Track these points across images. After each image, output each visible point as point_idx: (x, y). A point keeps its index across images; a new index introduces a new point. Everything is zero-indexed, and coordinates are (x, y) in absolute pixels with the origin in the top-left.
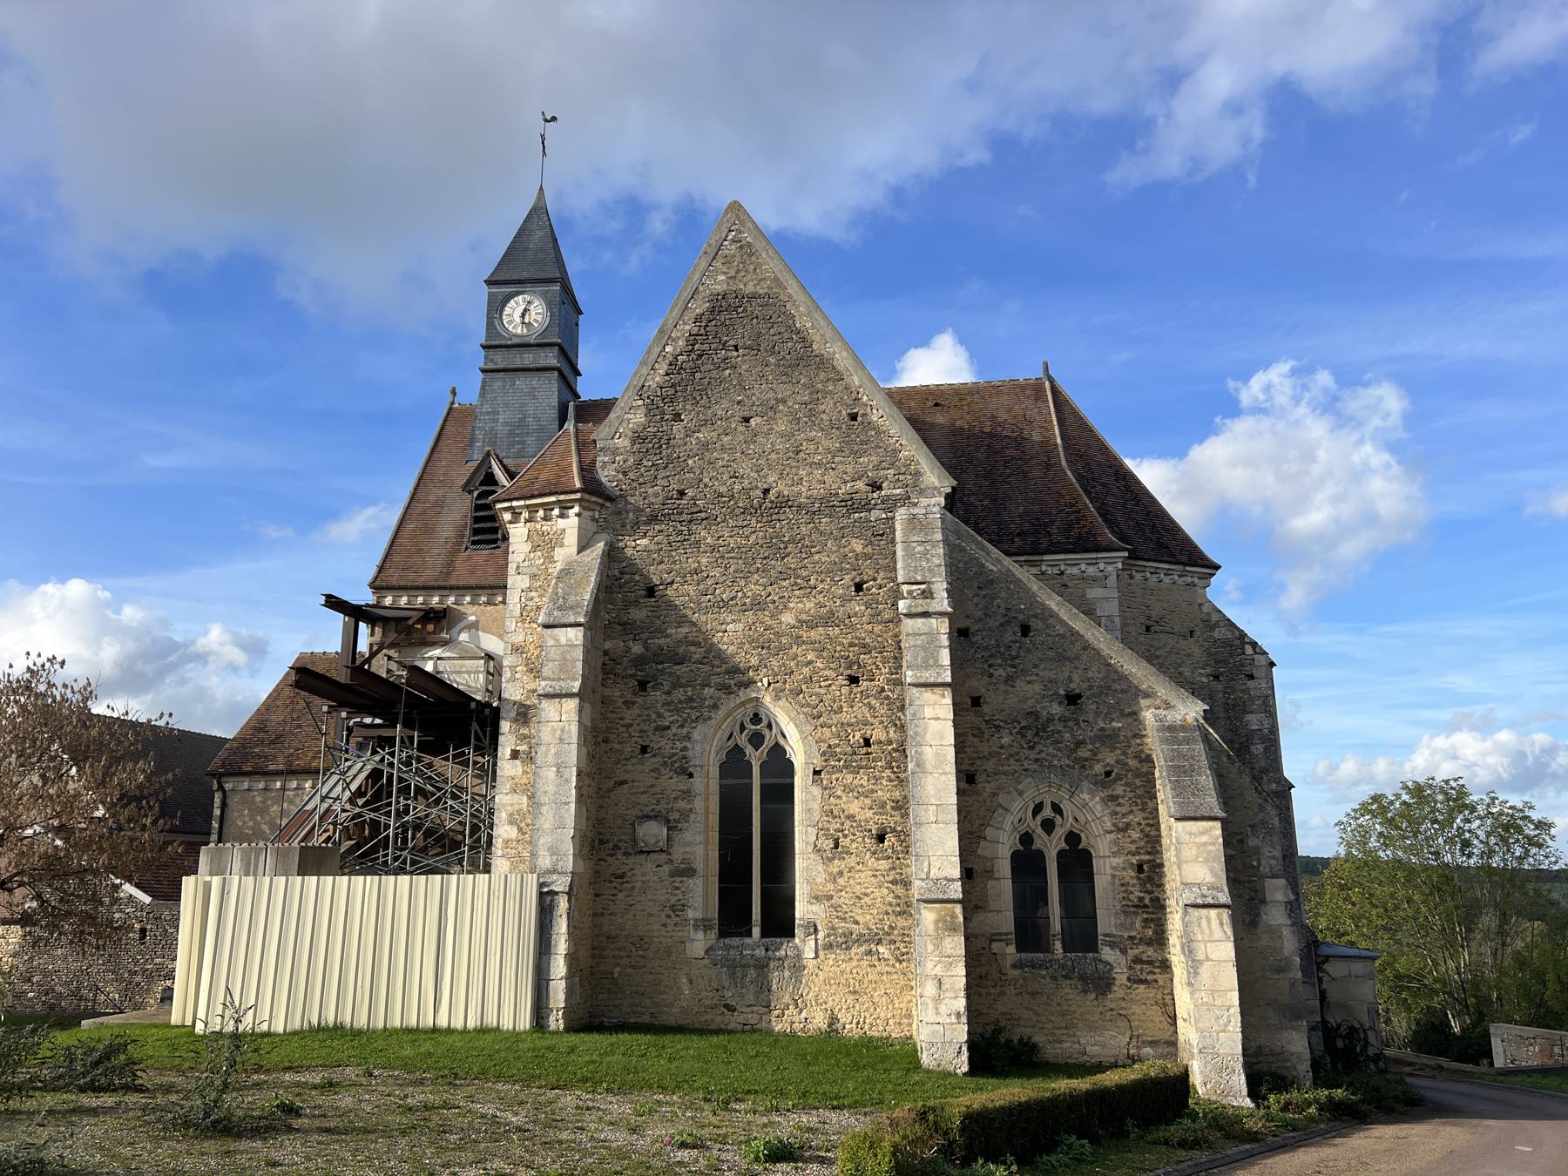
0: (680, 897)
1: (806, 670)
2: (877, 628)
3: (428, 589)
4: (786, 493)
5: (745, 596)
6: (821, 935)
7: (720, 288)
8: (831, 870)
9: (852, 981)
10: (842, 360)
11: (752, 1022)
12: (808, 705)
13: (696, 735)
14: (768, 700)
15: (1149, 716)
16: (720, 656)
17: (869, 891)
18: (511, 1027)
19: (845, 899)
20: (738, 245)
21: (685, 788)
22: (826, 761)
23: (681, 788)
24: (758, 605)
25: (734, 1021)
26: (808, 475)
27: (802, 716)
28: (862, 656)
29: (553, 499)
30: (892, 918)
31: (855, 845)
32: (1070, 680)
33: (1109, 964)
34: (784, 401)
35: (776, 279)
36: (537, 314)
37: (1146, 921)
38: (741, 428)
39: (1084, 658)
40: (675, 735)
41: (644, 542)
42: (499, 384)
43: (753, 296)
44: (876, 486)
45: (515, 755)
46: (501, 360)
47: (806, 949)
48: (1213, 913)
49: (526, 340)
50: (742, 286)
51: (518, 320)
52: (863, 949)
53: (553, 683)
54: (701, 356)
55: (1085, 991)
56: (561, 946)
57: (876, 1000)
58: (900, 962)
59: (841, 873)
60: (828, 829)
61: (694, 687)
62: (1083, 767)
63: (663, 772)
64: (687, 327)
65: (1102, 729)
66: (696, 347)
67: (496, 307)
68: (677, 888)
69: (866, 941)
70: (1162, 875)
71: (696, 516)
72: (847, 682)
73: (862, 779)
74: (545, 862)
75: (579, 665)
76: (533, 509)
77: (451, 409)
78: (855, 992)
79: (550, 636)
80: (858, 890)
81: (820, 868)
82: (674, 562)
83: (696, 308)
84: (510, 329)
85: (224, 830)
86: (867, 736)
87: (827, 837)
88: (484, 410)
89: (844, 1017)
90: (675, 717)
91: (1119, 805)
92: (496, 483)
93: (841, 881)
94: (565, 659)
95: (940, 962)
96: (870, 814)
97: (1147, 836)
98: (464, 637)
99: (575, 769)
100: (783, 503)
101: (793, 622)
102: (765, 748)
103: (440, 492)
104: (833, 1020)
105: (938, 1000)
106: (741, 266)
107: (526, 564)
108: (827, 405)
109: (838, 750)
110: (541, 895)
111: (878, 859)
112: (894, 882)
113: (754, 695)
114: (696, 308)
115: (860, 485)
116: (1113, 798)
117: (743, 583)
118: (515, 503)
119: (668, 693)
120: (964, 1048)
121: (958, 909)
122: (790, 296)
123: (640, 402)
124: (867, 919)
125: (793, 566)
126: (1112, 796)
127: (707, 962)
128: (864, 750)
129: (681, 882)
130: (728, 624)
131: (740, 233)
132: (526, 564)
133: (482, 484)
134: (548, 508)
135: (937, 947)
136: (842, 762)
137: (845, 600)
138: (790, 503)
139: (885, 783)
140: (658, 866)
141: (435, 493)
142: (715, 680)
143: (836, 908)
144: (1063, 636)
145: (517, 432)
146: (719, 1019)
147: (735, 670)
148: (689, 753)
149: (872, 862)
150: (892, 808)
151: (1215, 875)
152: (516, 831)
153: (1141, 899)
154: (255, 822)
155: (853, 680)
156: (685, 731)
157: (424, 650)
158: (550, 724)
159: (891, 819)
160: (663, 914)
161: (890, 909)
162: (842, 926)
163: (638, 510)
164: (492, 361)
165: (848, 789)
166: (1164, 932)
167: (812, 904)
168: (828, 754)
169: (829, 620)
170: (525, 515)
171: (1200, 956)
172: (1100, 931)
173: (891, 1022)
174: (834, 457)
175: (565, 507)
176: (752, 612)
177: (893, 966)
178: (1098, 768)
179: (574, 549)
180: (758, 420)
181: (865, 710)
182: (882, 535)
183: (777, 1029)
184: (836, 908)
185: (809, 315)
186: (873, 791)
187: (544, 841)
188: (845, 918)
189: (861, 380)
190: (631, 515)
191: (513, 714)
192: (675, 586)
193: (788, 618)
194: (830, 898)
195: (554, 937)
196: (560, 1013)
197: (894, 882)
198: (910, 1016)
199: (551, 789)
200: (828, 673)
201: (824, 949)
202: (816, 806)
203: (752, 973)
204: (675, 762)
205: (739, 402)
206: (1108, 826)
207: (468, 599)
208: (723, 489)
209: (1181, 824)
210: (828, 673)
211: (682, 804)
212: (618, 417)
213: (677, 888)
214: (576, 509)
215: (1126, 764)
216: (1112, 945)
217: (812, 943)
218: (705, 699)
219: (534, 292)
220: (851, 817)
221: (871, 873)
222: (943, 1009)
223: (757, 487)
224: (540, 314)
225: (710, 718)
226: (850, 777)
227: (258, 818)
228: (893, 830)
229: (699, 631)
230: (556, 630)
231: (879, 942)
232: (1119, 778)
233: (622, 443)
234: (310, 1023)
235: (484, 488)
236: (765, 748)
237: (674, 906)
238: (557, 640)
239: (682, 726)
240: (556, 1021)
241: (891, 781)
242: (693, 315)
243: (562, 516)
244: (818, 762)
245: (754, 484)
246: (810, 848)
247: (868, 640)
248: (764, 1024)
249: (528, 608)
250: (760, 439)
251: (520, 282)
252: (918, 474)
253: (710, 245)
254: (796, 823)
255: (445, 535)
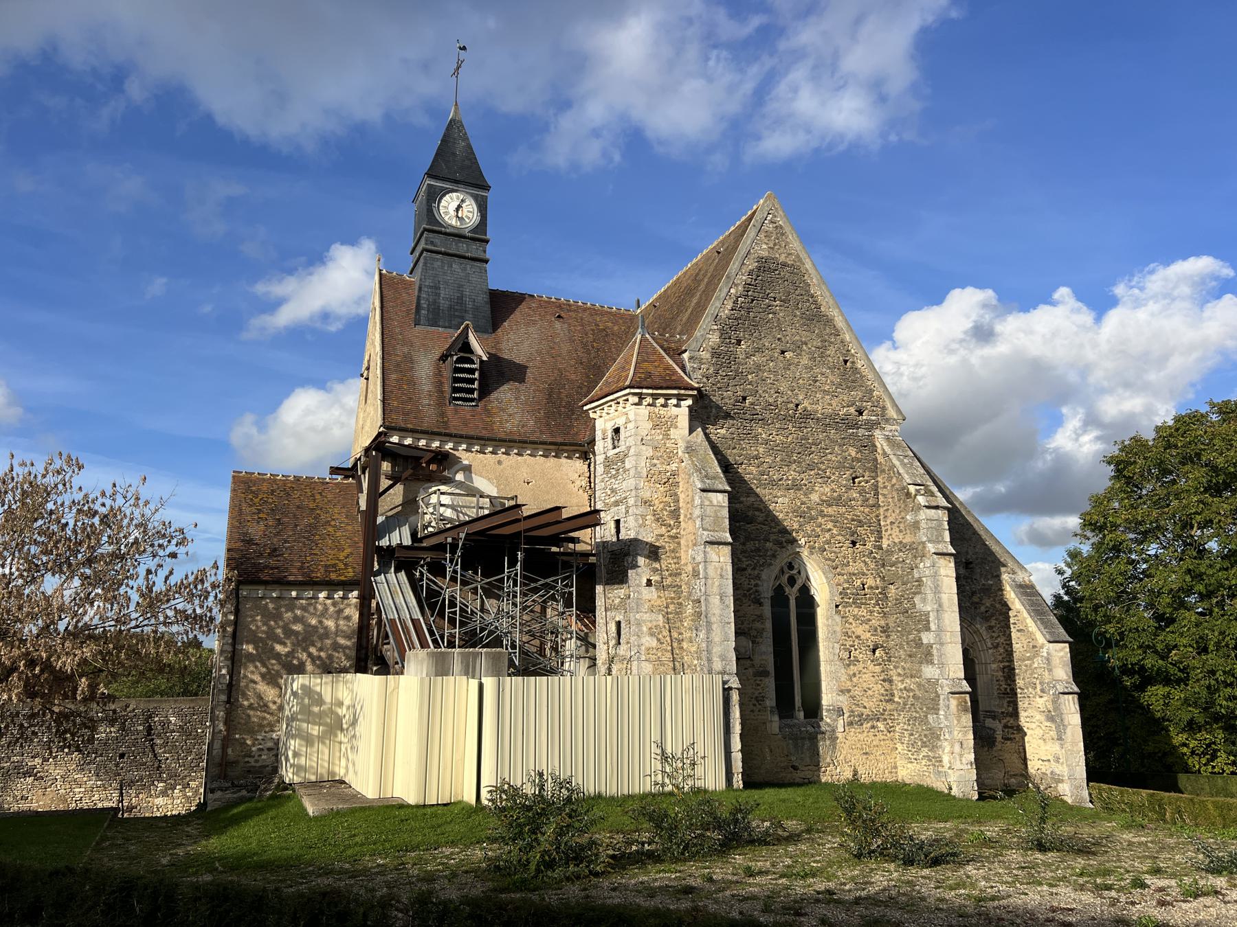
0: (761, 691)
1: (827, 535)
2: (867, 510)
3: (431, 434)
4: (809, 409)
5: (788, 479)
6: (846, 716)
7: (765, 254)
8: (848, 672)
9: (864, 746)
10: (839, 322)
11: (808, 777)
12: (830, 559)
13: (764, 577)
14: (805, 553)
15: (1005, 577)
16: (775, 520)
17: (871, 686)
18: (714, 789)
19: (857, 692)
20: (775, 225)
21: (758, 613)
22: (842, 598)
23: (756, 613)
24: (796, 486)
25: (798, 776)
26: (822, 398)
27: (827, 567)
28: (859, 528)
29: (675, 392)
30: (884, 704)
31: (861, 656)
32: (967, 553)
33: (991, 729)
34: (806, 344)
35: (798, 256)
36: (468, 211)
37: (1009, 702)
38: (781, 358)
39: (974, 539)
40: (750, 575)
41: (723, 431)
42: (439, 263)
43: (784, 265)
44: (861, 413)
45: (649, 583)
46: (440, 244)
47: (839, 726)
48: (1071, 696)
49: (461, 232)
50: (778, 256)
51: (453, 213)
52: (869, 725)
53: (712, 533)
54: (753, 300)
55: (983, 746)
56: (737, 728)
57: (878, 758)
58: (890, 732)
59: (854, 675)
60: (846, 645)
61: (759, 541)
62: (976, 608)
63: (744, 601)
64: (744, 278)
65: (984, 585)
66: (750, 293)
67: (434, 196)
68: (758, 685)
69: (872, 719)
70: (1014, 675)
71: (755, 418)
72: (851, 545)
73: (863, 612)
74: (718, 665)
75: (727, 522)
76: (655, 397)
77: (381, 274)
78: (866, 753)
79: (706, 498)
80: (865, 685)
81: (843, 671)
82: (742, 449)
83: (749, 265)
84: (446, 219)
85: (238, 634)
86: (864, 582)
87: (846, 650)
88: (427, 284)
89: (861, 771)
90: (750, 562)
91: (994, 632)
92: (472, 352)
93: (855, 679)
94: (717, 516)
95: (960, 731)
96: (868, 635)
97: (1007, 651)
98: (460, 477)
99: (732, 598)
100: (807, 415)
101: (818, 500)
102: (797, 587)
103: (406, 350)
104: (855, 773)
105: (961, 755)
106: (777, 241)
107: (649, 438)
108: (831, 351)
109: (849, 591)
110: (724, 689)
111: (875, 665)
112: (884, 680)
113: (798, 550)
114: (749, 265)
115: (852, 410)
116: (991, 628)
117: (786, 469)
118: (645, 391)
119: (744, 544)
120: (975, 784)
121: (968, 697)
122: (807, 270)
123: (716, 327)
124: (871, 705)
125: (816, 461)
126: (990, 626)
127: (780, 736)
128: (863, 592)
129: (761, 680)
130: (779, 498)
131: (775, 216)
132: (649, 438)
133: (460, 350)
134: (667, 397)
135: (958, 721)
136: (851, 600)
137: (849, 489)
138: (812, 416)
139: (876, 614)
140: (746, 669)
141: (401, 350)
142: (772, 537)
143: (853, 697)
144: (963, 525)
145: (456, 307)
146: (789, 776)
147: (785, 531)
148: (760, 589)
149: (871, 667)
150: (881, 631)
151: (1067, 675)
152: (656, 642)
153: (1006, 689)
154: (269, 627)
155: (854, 543)
156: (756, 572)
157: (426, 485)
158: (714, 564)
159: (880, 639)
160: (751, 703)
161: (882, 698)
162: (858, 710)
163: (719, 408)
164: (432, 243)
165: (856, 618)
166: (1017, 708)
167: (839, 695)
168: (843, 594)
169: (837, 501)
170: (649, 400)
171: (1066, 723)
172: (981, 708)
173: (886, 771)
174: (836, 388)
175: (680, 398)
176: (792, 491)
177: (886, 735)
178: (983, 609)
179: (687, 431)
180: (792, 354)
181: (863, 565)
182: (865, 447)
183: (823, 781)
184: (853, 697)
185: (819, 286)
186: (870, 620)
187: (716, 650)
188: (858, 705)
189: (850, 338)
190: (714, 410)
191: (646, 552)
192: (743, 466)
193: (815, 497)
194: (849, 691)
195: (732, 721)
196: (740, 776)
197: (884, 680)
198: (896, 767)
199: (717, 612)
200: (840, 538)
201: (848, 725)
202: (838, 629)
203: (807, 743)
204: (751, 594)
205: (779, 339)
206: (989, 645)
207: (464, 446)
208: (771, 400)
209: (1051, 645)
210: (840, 538)
211: (758, 625)
212: (702, 335)
213: (758, 685)
214: (689, 402)
215: (995, 607)
216: (994, 718)
217: (842, 721)
218: (767, 550)
219: (467, 193)
220: (858, 637)
221: (871, 674)
222: (964, 761)
223: (792, 402)
224: (471, 212)
225: (771, 564)
226: (856, 610)
227: (272, 623)
228: (882, 646)
229: (761, 501)
230: (710, 494)
231: (878, 720)
232: (992, 615)
233: (705, 355)
234: (588, 790)
235: (462, 354)
236: (797, 587)
237: (757, 697)
238: (711, 502)
239: (754, 569)
240: (738, 782)
241: (880, 613)
242: (748, 270)
243: (678, 406)
244: (838, 599)
245: (790, 399)
246: (837, 657)
247: (862, 518)
248: (816, 778)
249: (652, 472)
250: (792, 367)
251: (456, 182)
252: (884, 408)
253: (757, 221)
254: (820, 640)
255: (426, 388)
